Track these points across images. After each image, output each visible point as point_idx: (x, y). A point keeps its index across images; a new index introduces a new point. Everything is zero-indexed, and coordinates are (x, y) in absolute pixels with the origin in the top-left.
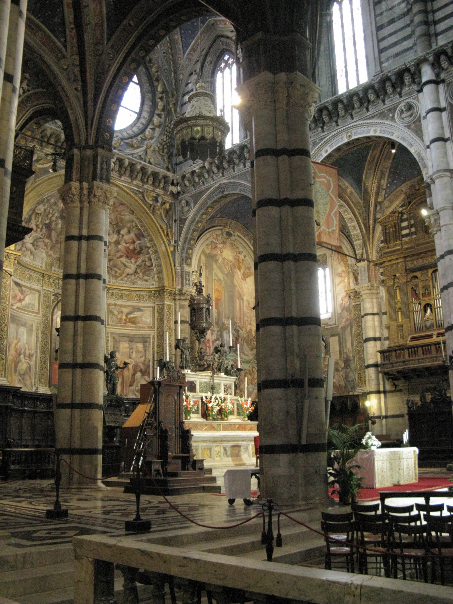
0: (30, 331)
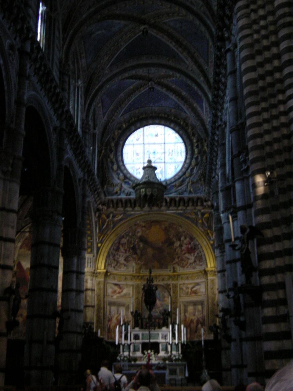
0: (128, 308)
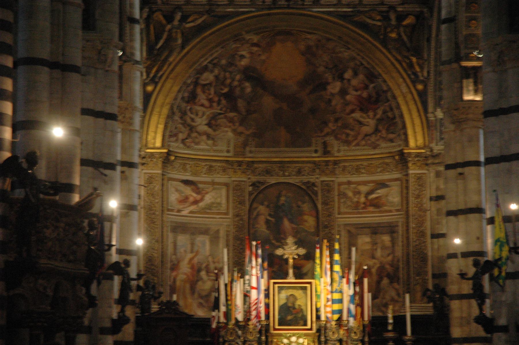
0: (215, 239)
